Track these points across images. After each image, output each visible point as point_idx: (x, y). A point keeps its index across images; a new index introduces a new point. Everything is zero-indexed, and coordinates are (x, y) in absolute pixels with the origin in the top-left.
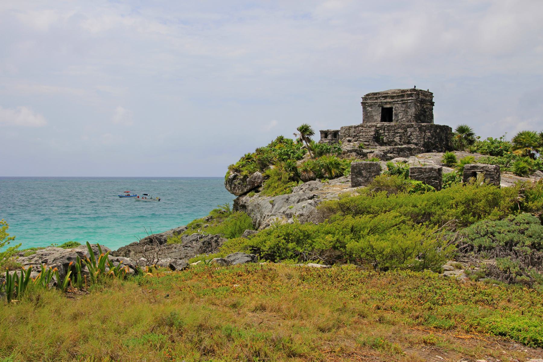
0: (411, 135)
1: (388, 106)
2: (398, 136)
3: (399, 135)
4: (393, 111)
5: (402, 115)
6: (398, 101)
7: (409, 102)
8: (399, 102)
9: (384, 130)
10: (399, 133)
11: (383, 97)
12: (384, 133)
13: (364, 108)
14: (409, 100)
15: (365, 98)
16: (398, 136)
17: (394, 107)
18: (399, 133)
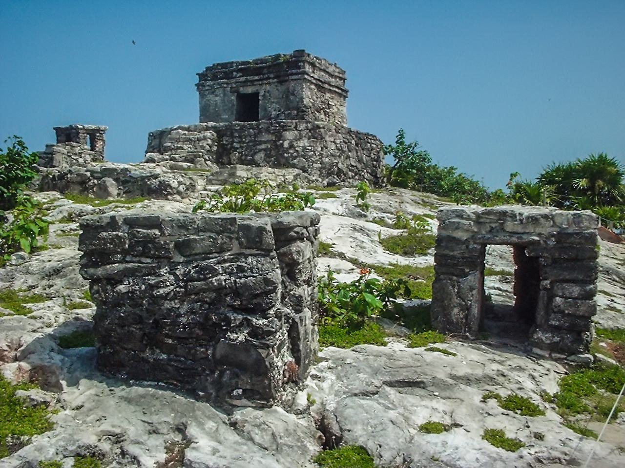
0: (291, 146)
1: (250, 90)
2: (260, 150)
3: (263, 146)
4: (259, 100)
5: (277, 109)
6: (270, 78)
7: (292, 80)
8: (271, 81)
9: (232, 136)
10: (265, 142)
11: (239, 71)
12: (233, 142)
13: (202, 96)
14: (292, 74)
15: (202, 76)
16: (260, 150)
17: (262, 93)
18: (265, 142)
